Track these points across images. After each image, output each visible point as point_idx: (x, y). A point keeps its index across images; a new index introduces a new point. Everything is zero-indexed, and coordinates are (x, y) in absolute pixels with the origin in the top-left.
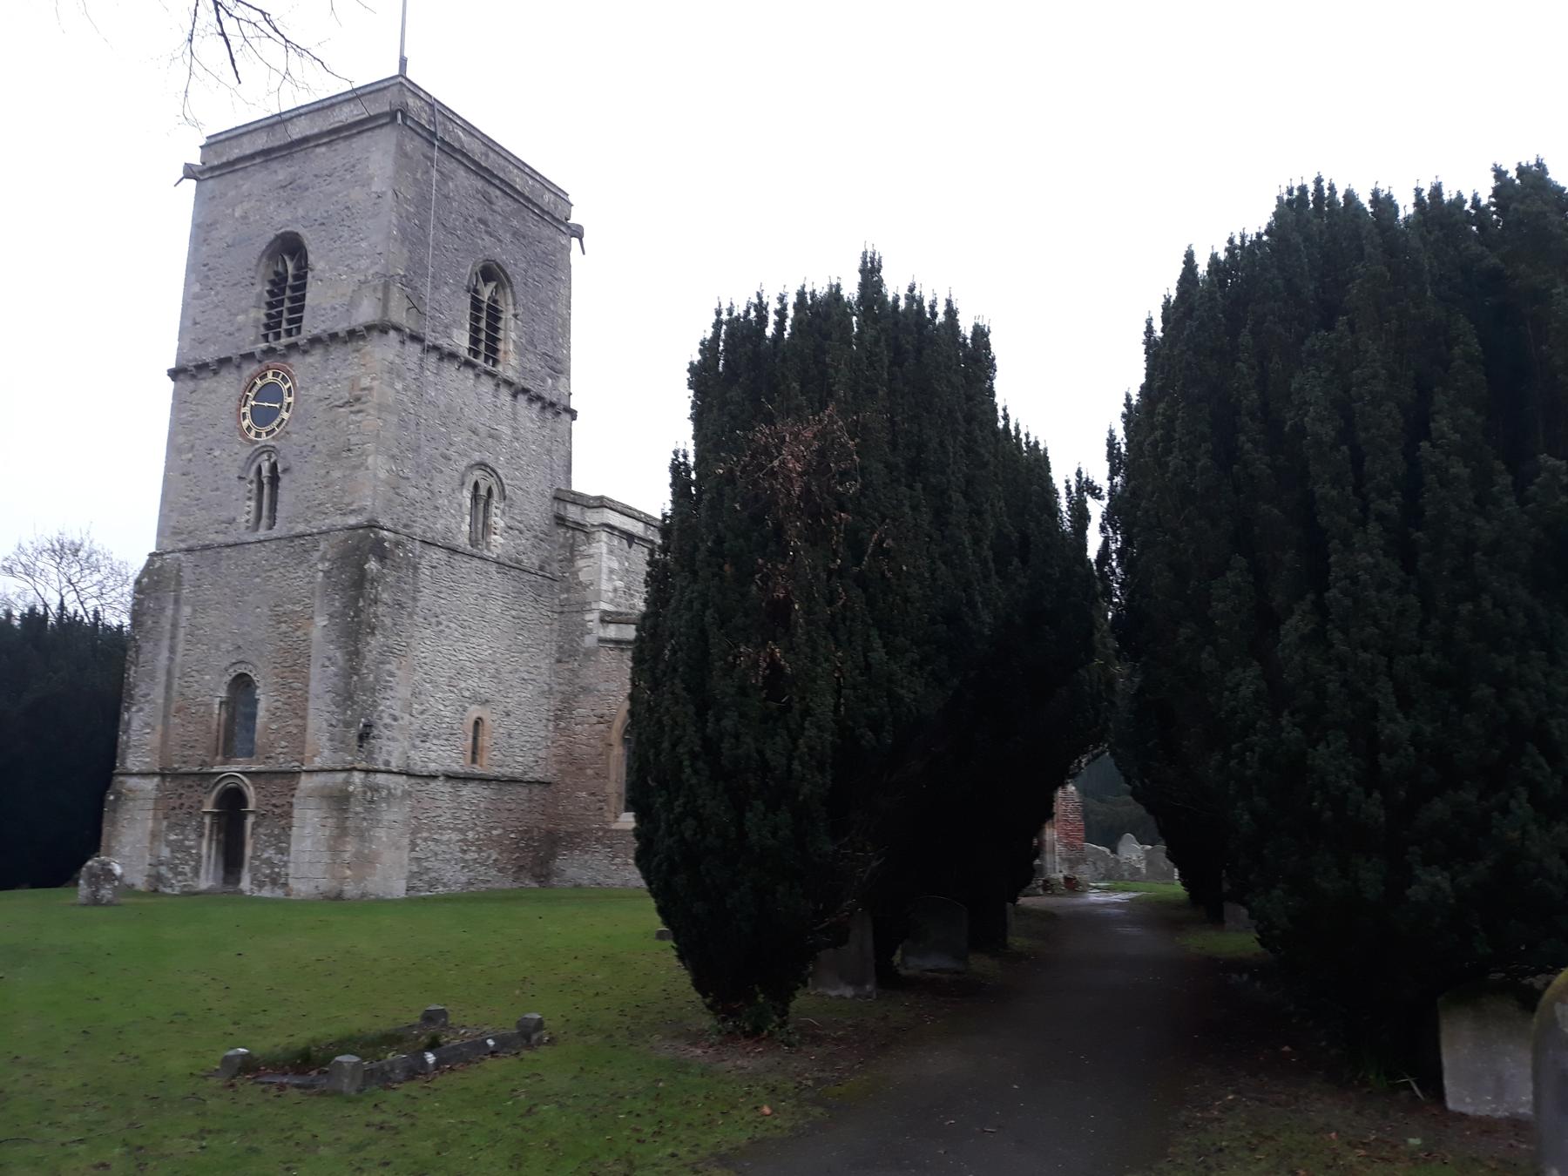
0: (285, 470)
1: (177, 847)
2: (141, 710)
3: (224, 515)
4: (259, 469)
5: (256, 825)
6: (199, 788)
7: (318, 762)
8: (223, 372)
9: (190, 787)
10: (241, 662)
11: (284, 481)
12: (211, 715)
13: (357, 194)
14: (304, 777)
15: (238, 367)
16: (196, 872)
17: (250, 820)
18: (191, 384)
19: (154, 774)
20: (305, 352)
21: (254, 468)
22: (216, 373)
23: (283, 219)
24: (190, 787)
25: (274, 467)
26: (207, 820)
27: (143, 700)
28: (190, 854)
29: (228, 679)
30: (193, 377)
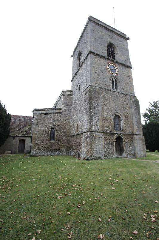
0: (119, 82)
1: (107, 148)
2: (95, 118)
3: (107, 84)
4: (113, 79)
5: (125, 144)
6: (111, 136)
7: (136, 133)
8: (102, 58)
9: (108, 136)
10: (117, 113)
11: (118, 84)
12: (112, 122)
13: (122, 46)
14: (135, 135)
15: (105, 59)
16: (113, 153)
17: (124, 143)
18: (95, 57)
19: (102, 132)
20: (119, 64)
21: (112, 79)
22: (100, 57)
23: (110, 40)
24: (108, 136)
25: (116, 80)
26: (114, 143)
27: (96, 116)
28: (111, 150)
29: (115, 116)
30: (95, 55)
